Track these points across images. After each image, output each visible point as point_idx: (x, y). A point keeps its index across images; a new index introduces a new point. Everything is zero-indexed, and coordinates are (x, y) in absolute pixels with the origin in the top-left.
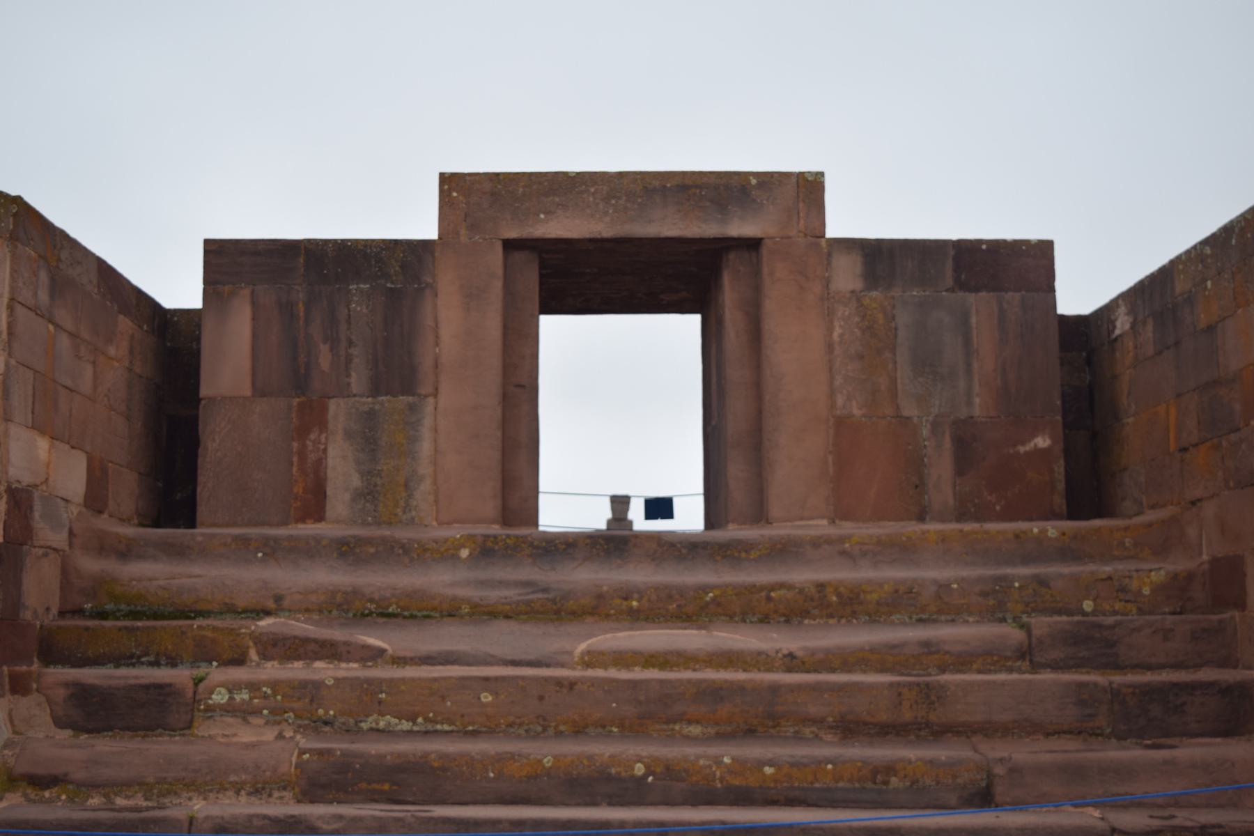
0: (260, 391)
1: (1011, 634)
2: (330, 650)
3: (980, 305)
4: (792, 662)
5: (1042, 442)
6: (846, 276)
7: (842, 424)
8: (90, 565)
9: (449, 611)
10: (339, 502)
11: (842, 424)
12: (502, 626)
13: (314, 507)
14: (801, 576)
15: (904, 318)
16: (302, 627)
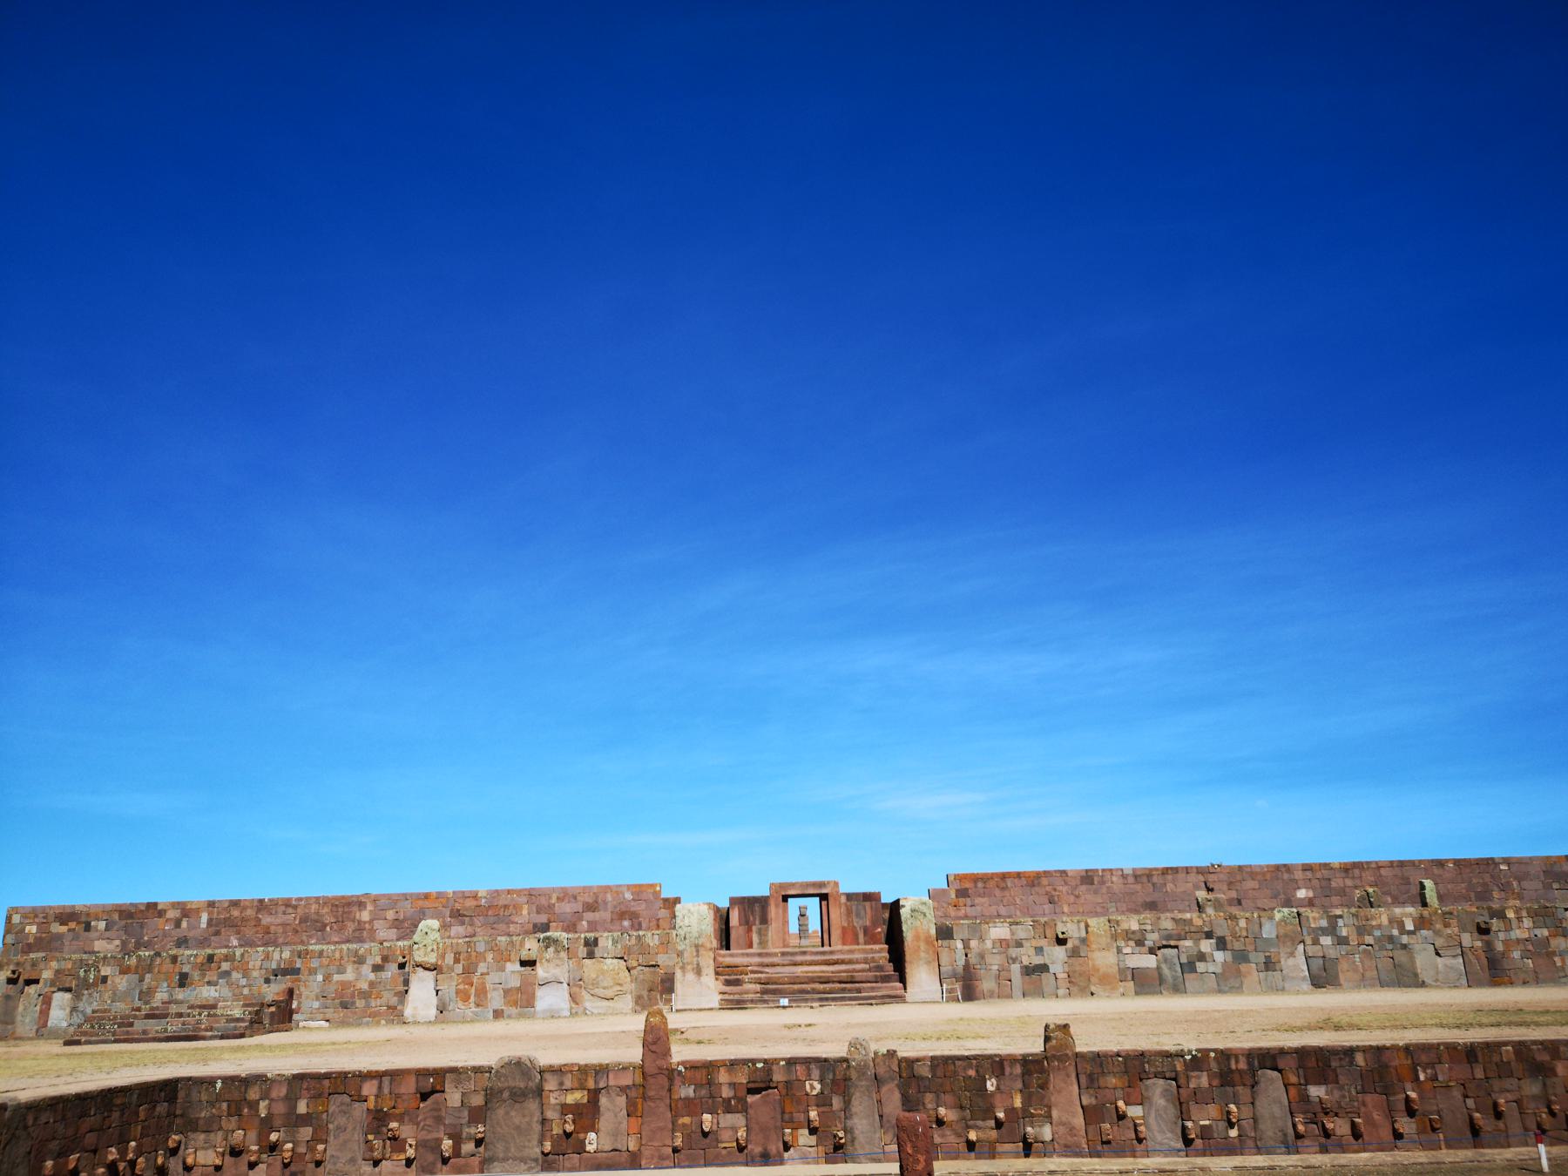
0: (740, 925)
1: (867, 966)
2: (761, 972)
3: (867, 904)
4: (832, 972)
5: (879, 930)
6: (843, 899)
7: (843, 928)
8: (721, 959)
9: (773, 965)
10: (755, 945)
11: (843, 928)
12: (787, 967)
13: (751, 946)
14: (835, 957)
15: (854, 908)
16: (756, 968)
